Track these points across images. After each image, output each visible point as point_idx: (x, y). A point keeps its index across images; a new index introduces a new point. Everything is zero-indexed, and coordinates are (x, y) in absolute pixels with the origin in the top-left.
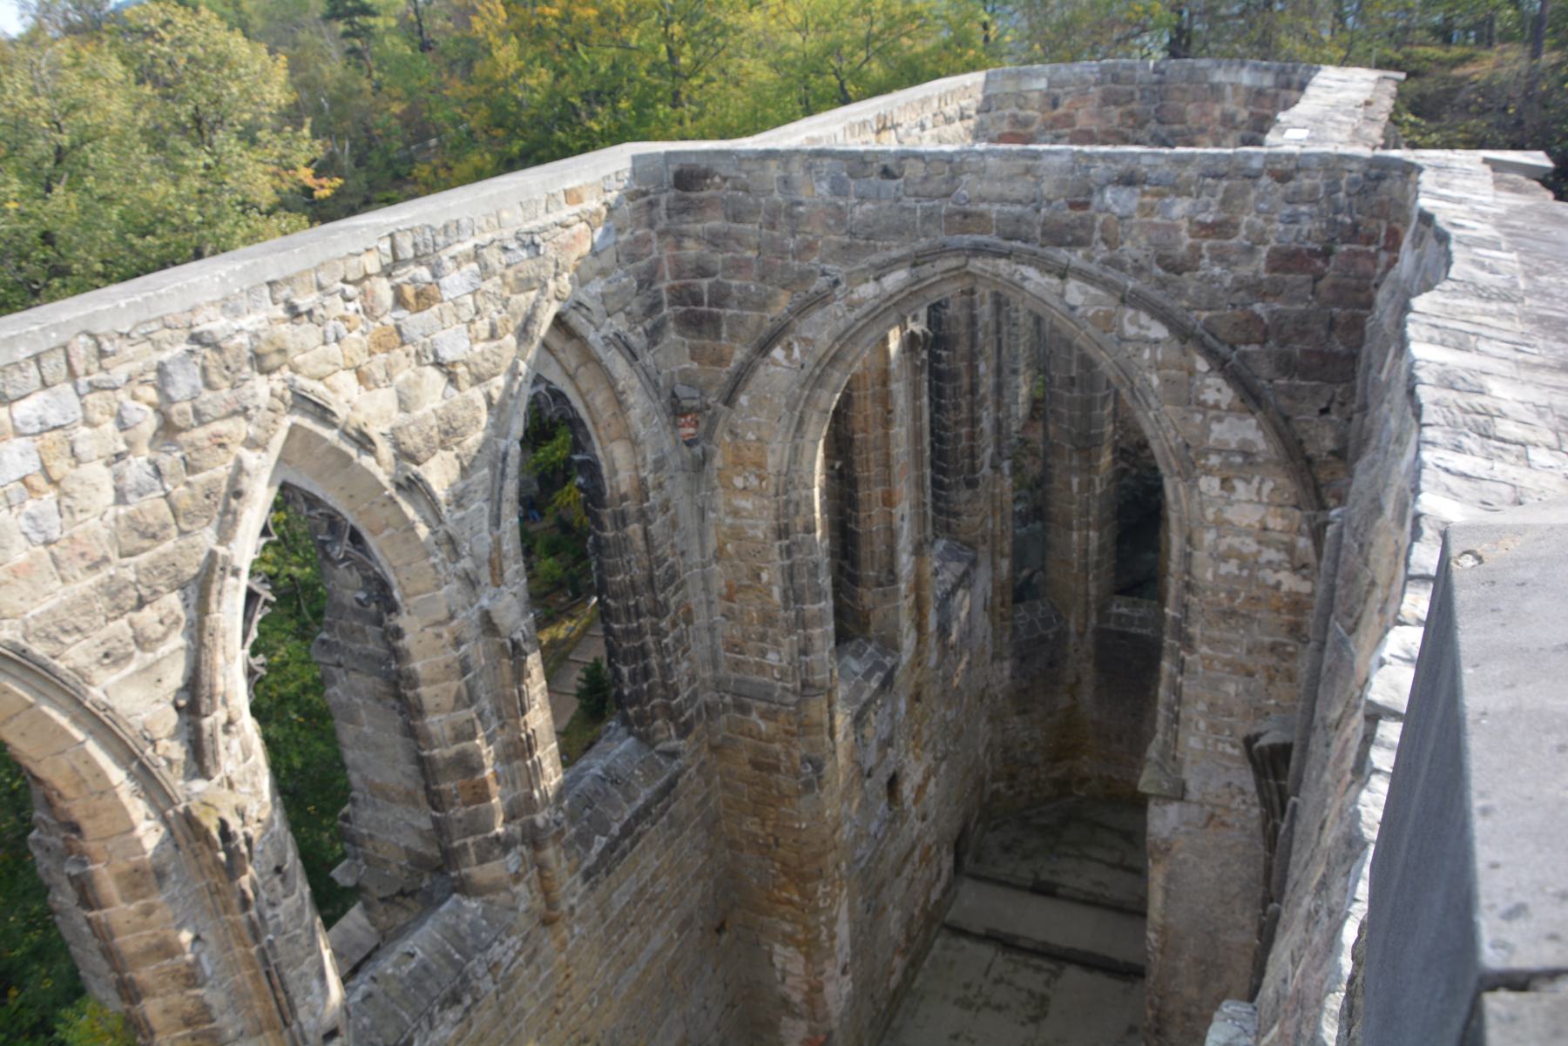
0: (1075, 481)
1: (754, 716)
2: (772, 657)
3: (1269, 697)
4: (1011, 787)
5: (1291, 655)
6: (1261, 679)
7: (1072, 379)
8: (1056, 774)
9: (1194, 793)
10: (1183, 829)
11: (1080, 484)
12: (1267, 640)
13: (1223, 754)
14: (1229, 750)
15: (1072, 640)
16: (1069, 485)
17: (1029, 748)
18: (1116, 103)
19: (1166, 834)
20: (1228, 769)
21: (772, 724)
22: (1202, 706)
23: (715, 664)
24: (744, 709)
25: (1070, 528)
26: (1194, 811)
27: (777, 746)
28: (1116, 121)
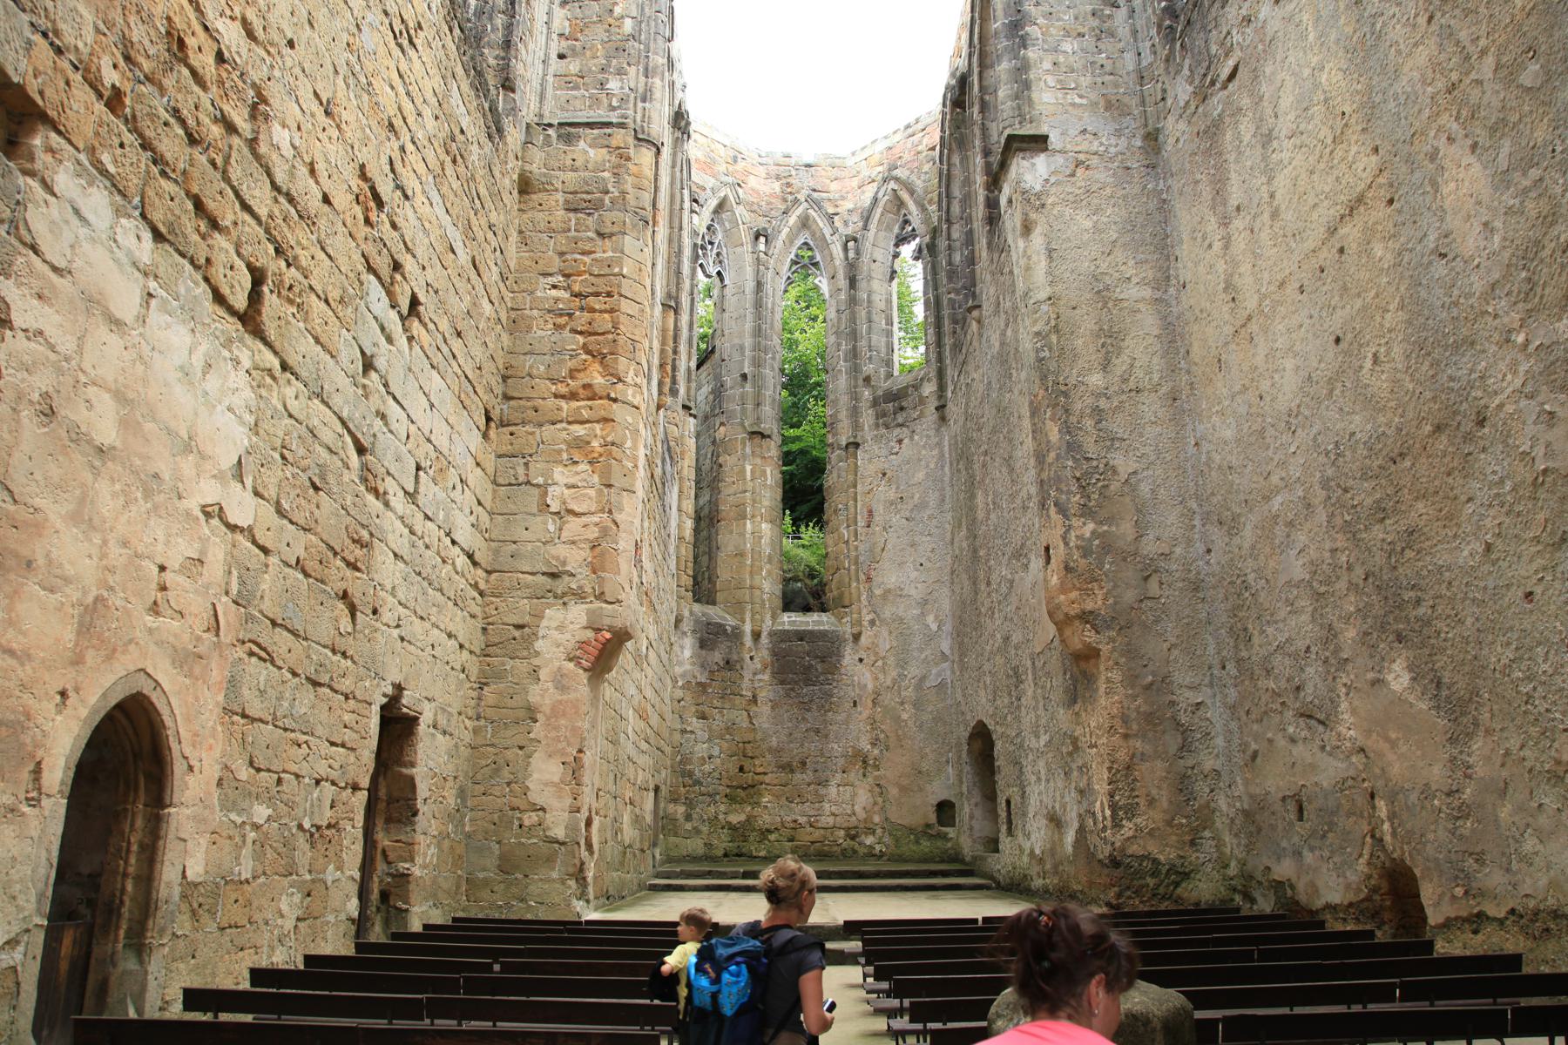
0: (748, 468)
1: (582, 143)
2: (614, 85)
3: (1100, 52)
4: (688, 818)
5: (1109, 16)
6: (1089, 41)
7: (744, 376)
8: (735, 819)
9: (1055, 140)
10: (1053, 180)
11: (752, 472)
12: (1089, 8)
13: (1073, 105)
14: (1078, 100)
15: (748, 641)
16: (743, 471)
17: (707, 768)
18: (778, 178)
19: (1038, 188)
20: (1080, 119)
21: (605, 151)
22: (1047, 65)
23: (542, 97)
24: (568, 139)
25: (745, 517)
26: (1059, 159)
27: (606, 174)
28: (778, 189)
